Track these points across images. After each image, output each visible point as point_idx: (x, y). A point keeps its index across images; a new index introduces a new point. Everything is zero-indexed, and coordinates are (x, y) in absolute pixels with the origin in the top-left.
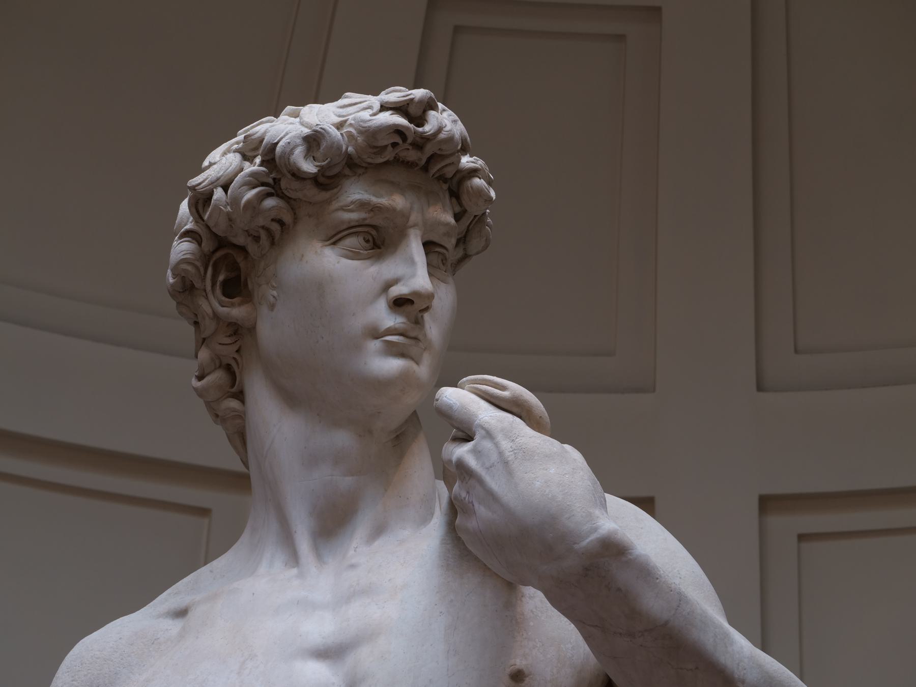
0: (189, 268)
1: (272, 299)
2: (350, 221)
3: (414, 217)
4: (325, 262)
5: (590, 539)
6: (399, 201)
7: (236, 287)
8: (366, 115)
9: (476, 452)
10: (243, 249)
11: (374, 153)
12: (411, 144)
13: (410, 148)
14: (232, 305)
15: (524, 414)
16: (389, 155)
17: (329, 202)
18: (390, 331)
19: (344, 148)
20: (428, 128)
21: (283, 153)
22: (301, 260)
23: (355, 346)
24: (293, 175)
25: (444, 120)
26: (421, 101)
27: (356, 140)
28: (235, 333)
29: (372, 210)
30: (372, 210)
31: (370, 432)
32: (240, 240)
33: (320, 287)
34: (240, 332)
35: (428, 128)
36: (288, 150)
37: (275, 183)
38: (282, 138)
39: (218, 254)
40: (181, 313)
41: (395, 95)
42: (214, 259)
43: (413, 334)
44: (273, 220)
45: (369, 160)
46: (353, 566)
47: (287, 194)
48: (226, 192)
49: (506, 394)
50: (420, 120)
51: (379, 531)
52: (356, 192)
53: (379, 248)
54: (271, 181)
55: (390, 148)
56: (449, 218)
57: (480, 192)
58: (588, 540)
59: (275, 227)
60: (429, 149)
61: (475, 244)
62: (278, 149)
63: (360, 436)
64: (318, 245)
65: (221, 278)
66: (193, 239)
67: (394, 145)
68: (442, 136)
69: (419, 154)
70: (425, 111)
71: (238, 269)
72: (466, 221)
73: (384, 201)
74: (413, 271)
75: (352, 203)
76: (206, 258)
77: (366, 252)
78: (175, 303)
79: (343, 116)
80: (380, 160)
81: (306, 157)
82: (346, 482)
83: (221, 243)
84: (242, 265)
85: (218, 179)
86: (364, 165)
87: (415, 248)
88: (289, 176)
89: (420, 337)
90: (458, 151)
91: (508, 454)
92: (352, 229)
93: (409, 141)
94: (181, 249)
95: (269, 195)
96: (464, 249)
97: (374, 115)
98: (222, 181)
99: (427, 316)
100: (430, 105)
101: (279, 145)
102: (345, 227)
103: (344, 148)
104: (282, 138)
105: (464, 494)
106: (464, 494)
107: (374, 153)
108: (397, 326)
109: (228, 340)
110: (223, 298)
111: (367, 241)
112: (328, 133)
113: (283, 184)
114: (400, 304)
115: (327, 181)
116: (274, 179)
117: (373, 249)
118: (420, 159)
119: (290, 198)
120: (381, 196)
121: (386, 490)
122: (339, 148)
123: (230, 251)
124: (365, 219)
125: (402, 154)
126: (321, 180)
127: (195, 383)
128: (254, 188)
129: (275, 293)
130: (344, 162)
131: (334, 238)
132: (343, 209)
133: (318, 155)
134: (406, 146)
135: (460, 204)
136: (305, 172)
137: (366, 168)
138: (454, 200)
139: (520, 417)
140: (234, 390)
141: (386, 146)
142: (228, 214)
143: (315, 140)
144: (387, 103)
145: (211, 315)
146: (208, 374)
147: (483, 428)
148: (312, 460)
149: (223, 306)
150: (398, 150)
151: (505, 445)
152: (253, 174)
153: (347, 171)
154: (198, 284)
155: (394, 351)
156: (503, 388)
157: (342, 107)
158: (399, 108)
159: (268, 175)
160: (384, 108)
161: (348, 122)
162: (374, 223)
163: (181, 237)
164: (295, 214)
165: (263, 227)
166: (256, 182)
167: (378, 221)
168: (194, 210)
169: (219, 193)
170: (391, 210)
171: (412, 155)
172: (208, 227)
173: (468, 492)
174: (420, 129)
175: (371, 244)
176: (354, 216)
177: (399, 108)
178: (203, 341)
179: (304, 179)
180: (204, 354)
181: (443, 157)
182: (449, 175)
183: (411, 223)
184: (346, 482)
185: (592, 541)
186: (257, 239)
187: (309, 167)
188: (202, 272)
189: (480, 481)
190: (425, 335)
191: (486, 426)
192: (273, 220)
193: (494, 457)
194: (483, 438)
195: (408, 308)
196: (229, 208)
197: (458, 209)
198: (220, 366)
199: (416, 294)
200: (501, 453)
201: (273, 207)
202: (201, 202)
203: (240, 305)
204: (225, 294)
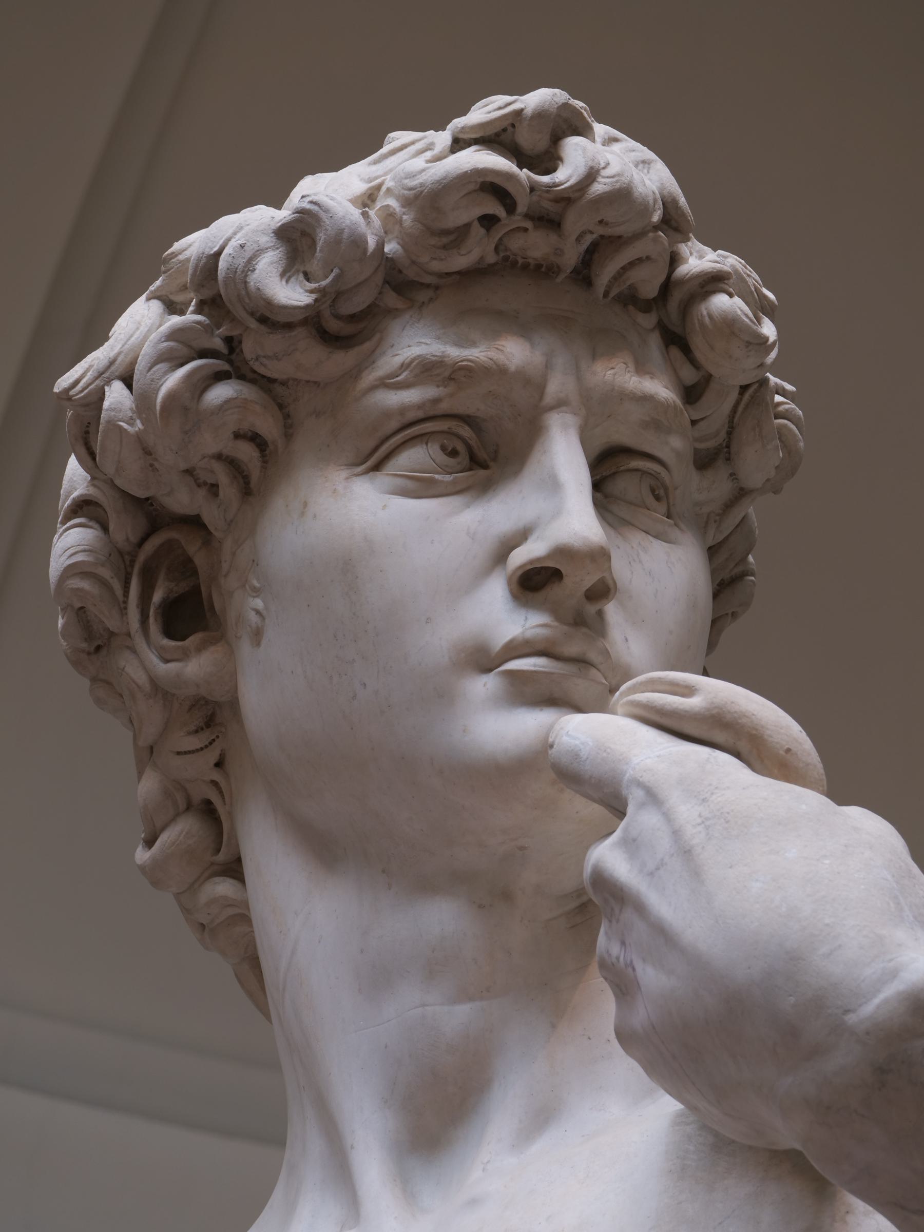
0: (85, 584)
1: (253, 618)
2: (403, 410)
3: (556, 386)
4: (355, 513)
5: (882, 996)
6: (513, 352)
7: (190, 614)
8: (419, 163)
9: (631, 845)
10: (195, 522)
11: (445, 247)
12: (527, 216)
13: (528, 224)
14: (184, 656)
15: (743, 746)
16: (477, 250)
17: (355, 373)
18: (516, 649)
19: (372, 242)
20: (566, 175)
21: (232, 270)
22: (303, 514)
23: (439, 695)
24: (263, 320)
25: (612, 158)
26: (540, 115)
27: (400, 222)
28: (210, 722)
29: (450, 378)
30: (450, 378)
31: (507, 896)
32: (182, 500)
33: (347, 568)
34: (213, 715)
35: (566, 175)
36: (241, 262)
37: (232, 350)
38: (229, 240)
40: (98, 701)
41: (485, 111)
42: (141, 558)
43: (572, 649)
44: (237, 436)
45: (436, 266)
46: (474, 1202)
47: (262, 370)
48: (129, 386)
49: (694, 703)
50: (547, 160)
51: (542, 1117)
52: (414, 342)
53: (484, 466)
54: (217, 343)
55: (478, 231)
56: (660, 389)
57: (729, 326)
58: (877, 1001)
59: (246, 452)
60: (575, 222)
61: (756, 462)
62: (222, 264)
63: (481, 907)
64: (338, 476)
65: (158, 596)
66: (91, 518)
67: (488, 221)
68: (599, 187)
69: (553, 238)
70: (556, 139)
71: (195, 572)
72: (717, 408)
73: (478, 353)
74: (557, 502)
75: (404, 366)
76: (122, 560)
77: (448, 478)
78: (86, 682)
79: (376, 178)
80: (461, 261)
81: (286, 274)
82: (456, 1017)
83: (152, 516)
84: (200, 560)
85: (112, 363)
86: (428, 279)
87: (564, 457)
88: (253, 324)
89: (593, 656)
90: (656, 228)
91: (694, 834)
92: (411, 428)
93: (521, 208)
94: (71, 542)
95: (219, 377)
96: (733, 476)
97: (438, 158)
98: (118, 368)
99: (612, 610)
100: (567, 124)
102: (394, 424)
103: (372, 242)
104: (229, 240)
105: (615, 949)
106: (615, 949)
107: (445, 247)
108: (529, 634)
109: (194, 742)
110: (166, 642)
111: (453, 453)
112: (327, 211)
113: (249, 348)
114: (533, 583)
115: (345, 323)
116: (229, 340)
117: (470, 469)
118: (559, 252)
119: (272, 381)
120: (473, 344)
121: (554, 1026)
122: (358, 242)
124: (436, 401)
125: (516, 244)
126: (333, 326)
127: (142, 855)
128: (182, 365)
129: (259, 603)
130: (379, 278)
131: (373, 460)
132: (385, 384)
133: (314, 266)
134: (517, 221)
135: (694, 363)
136: (285, 307)
137: (437, 288)
138: (675, 352)
139: (737, 755)
140: (221, 857)
141: (467, 226)
142: (139, 438)
143: (304, 234)
144: (463, 129)
145: (147, 687)
146: (163, 829)
147: (640, 784)
148: (377, 977)
149: (167, 661)
150: (498, 232)
151: (686, 812)
153: (391, 299)
156: (688, 691)
157: (375, 162)
158: (495, 138)
159: (207, 330)
160: (458, 144)
161: (384, 189)
162: (461, 410)
163: (67, 519)
164: (287, 416)
165: (219, 457)
166: (185, 351)
167: (469, 402)
169: (116, 395)
170: (497, 372)
171: (536, 245)
173: (623, 943)
174: (545, 179)
175: (464, 457)
176: (411, 396)
177: (495, 138)
178: (148, 755)
179: (289, 326)
181: (616, 242)
182: (650, 290)
183: (548, 399)
184: (456, 1017)
185: (886, 1001)
186: (214, 489)
187: (293, 295)
188: (119, 592)
189: (640, 908)
190: (606, 653)
191: (646, 778)
192: (237, 436)
193: (664, 844)
194: (642, 805)
195: (555, 592)
196: (139, 425)
197: (689, 375)
198: (189, 807)
200: (676, 834)
201: (228, 401)
203: (200, 649)
204: (170, 632)
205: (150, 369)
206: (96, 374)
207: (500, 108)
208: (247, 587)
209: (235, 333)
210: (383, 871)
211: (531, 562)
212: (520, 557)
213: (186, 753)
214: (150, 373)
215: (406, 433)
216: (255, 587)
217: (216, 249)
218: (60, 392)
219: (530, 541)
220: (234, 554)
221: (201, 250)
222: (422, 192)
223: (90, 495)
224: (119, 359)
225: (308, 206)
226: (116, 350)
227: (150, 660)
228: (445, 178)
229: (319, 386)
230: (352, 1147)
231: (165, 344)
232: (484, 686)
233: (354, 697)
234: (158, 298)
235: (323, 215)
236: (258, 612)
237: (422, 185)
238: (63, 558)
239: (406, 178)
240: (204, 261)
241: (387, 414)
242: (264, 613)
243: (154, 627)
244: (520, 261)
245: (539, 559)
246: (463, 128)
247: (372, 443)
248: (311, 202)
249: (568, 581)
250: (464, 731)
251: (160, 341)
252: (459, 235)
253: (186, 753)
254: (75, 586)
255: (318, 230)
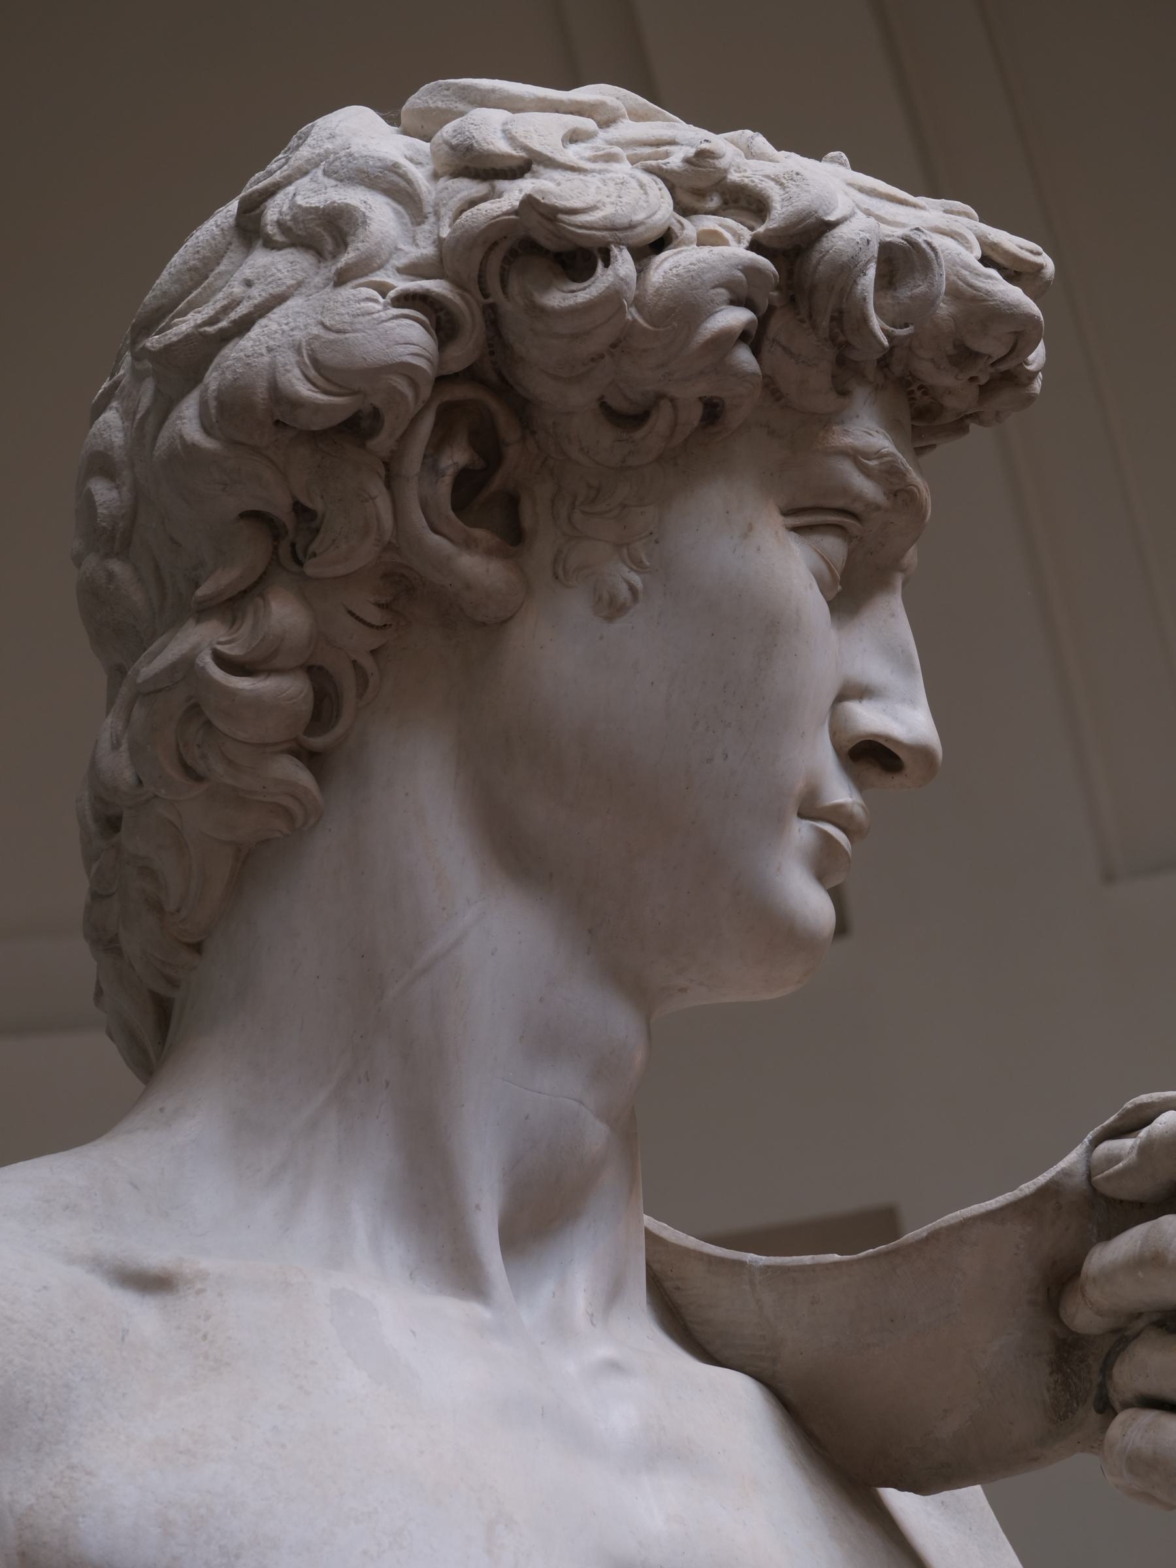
1: (624, 593)
2: (859, 497)
10: (523, 409)
13: (983, 380)
14: (468, 544)
17: (827, 420)
22: (745, 536)
39: (460, 392)
75: (879, 455)
82: (596, 1135)
84: (512, 453)
85: (631, 226)
88: (825, 323)
101: (837, 232)
102: (839, 503)
109: (375, 616)
110: (451, 513)
112: (940, 265)
113: (776, 325)
114: (871, 756)
123: (493, 404)
124: (878, 508)
129: (636, 579)
140: (317, 742)
144: (994, 246)
148: (546, 1040)
149: (436, 531)
152: (750, 270)
154: (382, 443)
155: (825, 864)
165: (672, 400)
168: (478, 255)
169: (624, 263)
172: (492, 317)
180: (284, 614)
199: (922, 752)
202: (505, 246)
203: (490, 553)
205: (714, 288)
206: (609, 225)
207: (1032, 252)
208: (625, 551)
209: (777, 304)
210: (590, 931)
211: (889, 739)
212: (870, 718)
213: (358, 618)
214: (713, 291)
215: (845, 520)
216: (641, 562)
217: (831, 218)
218: (545, 205)
219: (864, 702)
220: (624, 506)
221: (814, 207)
222: (985, 300)
223: (444, 296)
224: (640, 229)
225: (924, 246)
226: (640, 216)
227: (410, 510)
228: (1017, 307)
229: (778, 400)
230: (477, 1207)
231: (740, 274)
232: (802, 832)
233: (710, 760)
234: (665, 181)
235: (935, 266)
236: (632, 589)
237: (988, 293)
238: (401, 349)
239: (963, 267)
240: (812, 220)
241: (846, 490)
242: (641, 596)
243: (444, 488)
244: (914, 387)
245: (897, 743)
246: (995, 244)
247: (809, 503)
248: (929, 244)
249: (898, 779)
250: (779, 869)
251: (736, 266)
252: (963, 356)
253: (358, 618)
254: (400, 388)
255: (917, 275)
